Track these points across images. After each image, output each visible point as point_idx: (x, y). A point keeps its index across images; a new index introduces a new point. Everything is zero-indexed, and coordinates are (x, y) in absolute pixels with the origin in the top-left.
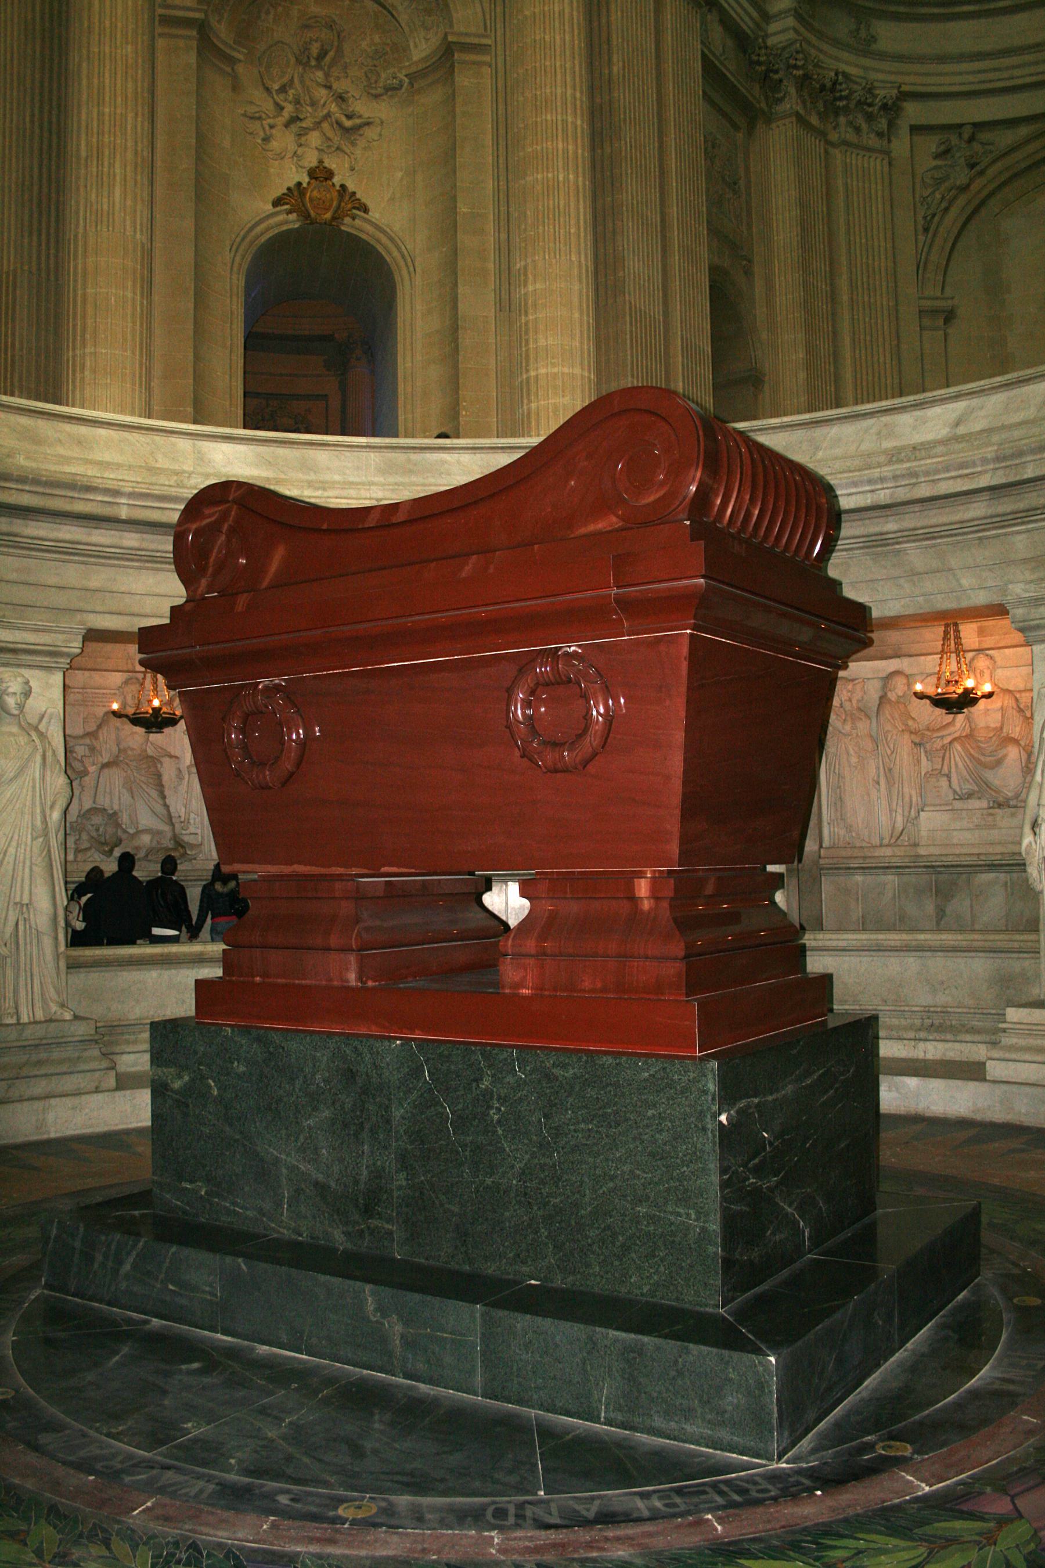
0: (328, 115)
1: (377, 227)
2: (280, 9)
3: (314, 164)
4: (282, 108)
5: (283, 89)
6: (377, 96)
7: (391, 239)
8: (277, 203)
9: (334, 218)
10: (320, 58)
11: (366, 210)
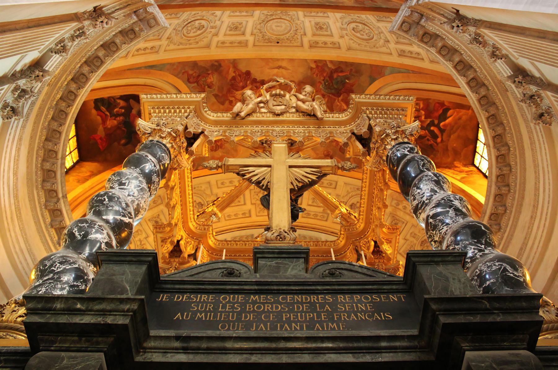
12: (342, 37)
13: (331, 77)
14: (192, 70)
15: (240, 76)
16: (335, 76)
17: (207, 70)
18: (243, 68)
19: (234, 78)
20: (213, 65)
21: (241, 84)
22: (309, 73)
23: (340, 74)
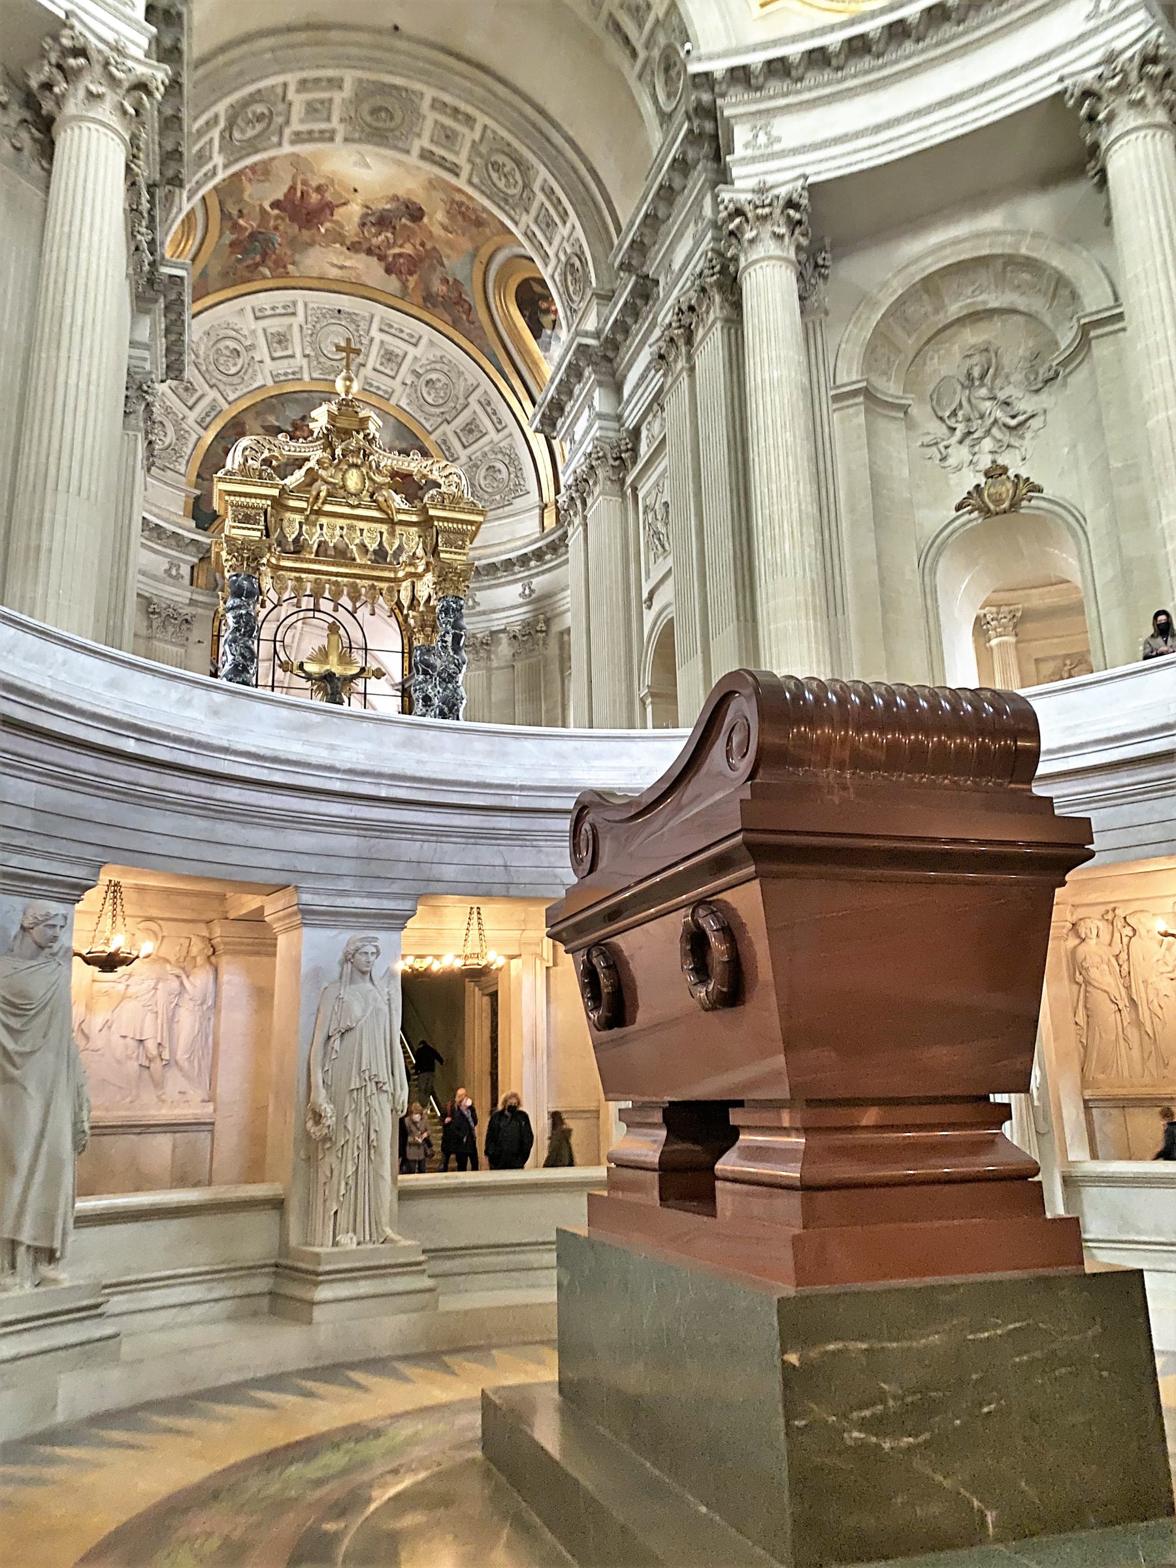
0: (996, 421)
1: (1050, 501)
2: (942, 352)
3: (989, 465)
4: (955, 429)
5: (954, 414)
6: (1037, 391)
7: (1065, 508)
8: (958, 509)
9: (1011, 506)
10: (982, 377)
11: (1040, 491)
12: (254, 331)
13: (265, 255)
14: (461, 318)
15: (401, 272)
16: (258, 258)
17: (442, 303)
18: (393, 283)
19: (411, 273)
20: (434, 306)
21: (401, 260)
22: (297, 257)
23: (250, 262)
